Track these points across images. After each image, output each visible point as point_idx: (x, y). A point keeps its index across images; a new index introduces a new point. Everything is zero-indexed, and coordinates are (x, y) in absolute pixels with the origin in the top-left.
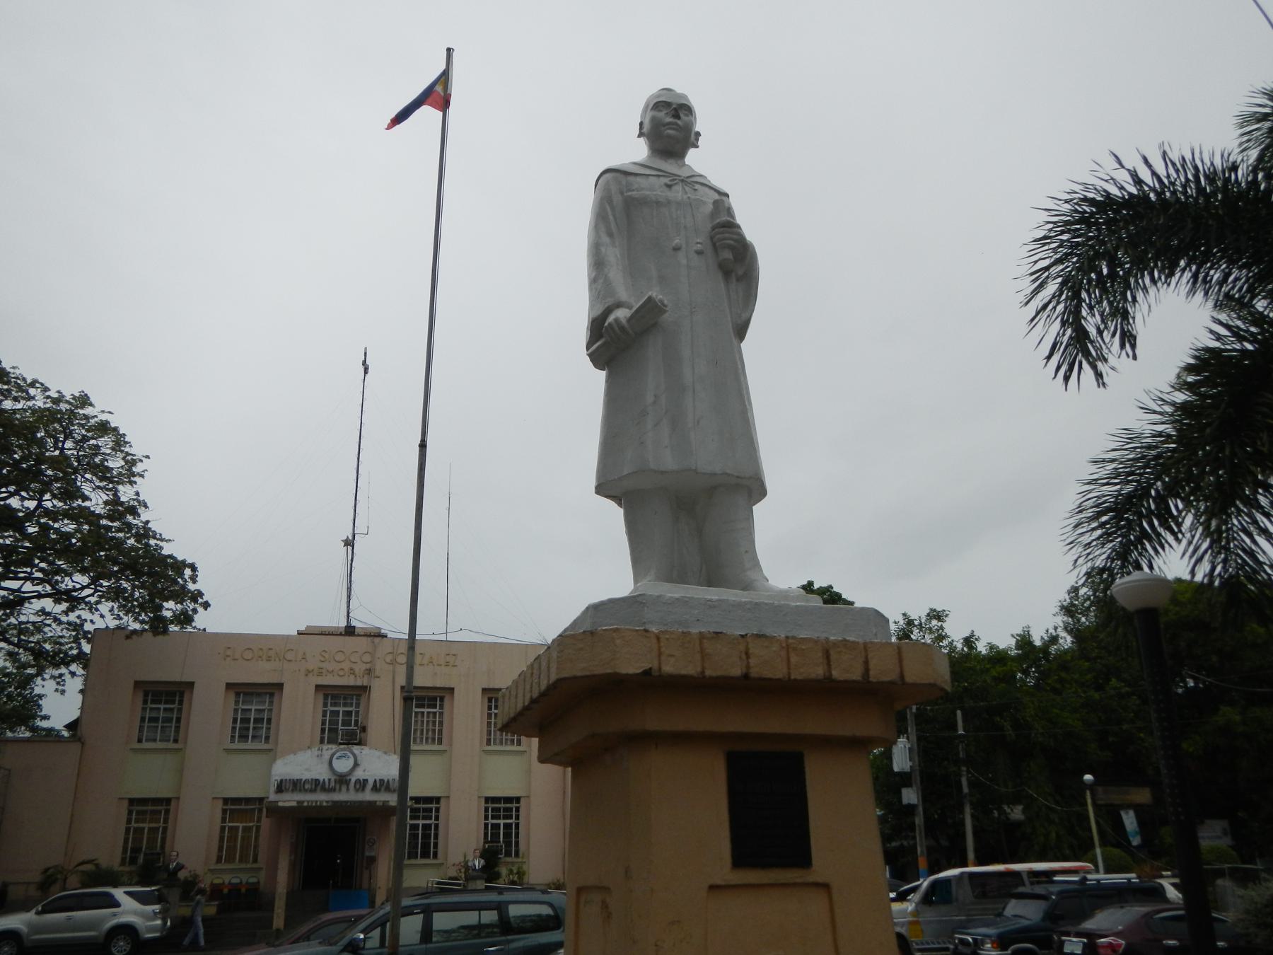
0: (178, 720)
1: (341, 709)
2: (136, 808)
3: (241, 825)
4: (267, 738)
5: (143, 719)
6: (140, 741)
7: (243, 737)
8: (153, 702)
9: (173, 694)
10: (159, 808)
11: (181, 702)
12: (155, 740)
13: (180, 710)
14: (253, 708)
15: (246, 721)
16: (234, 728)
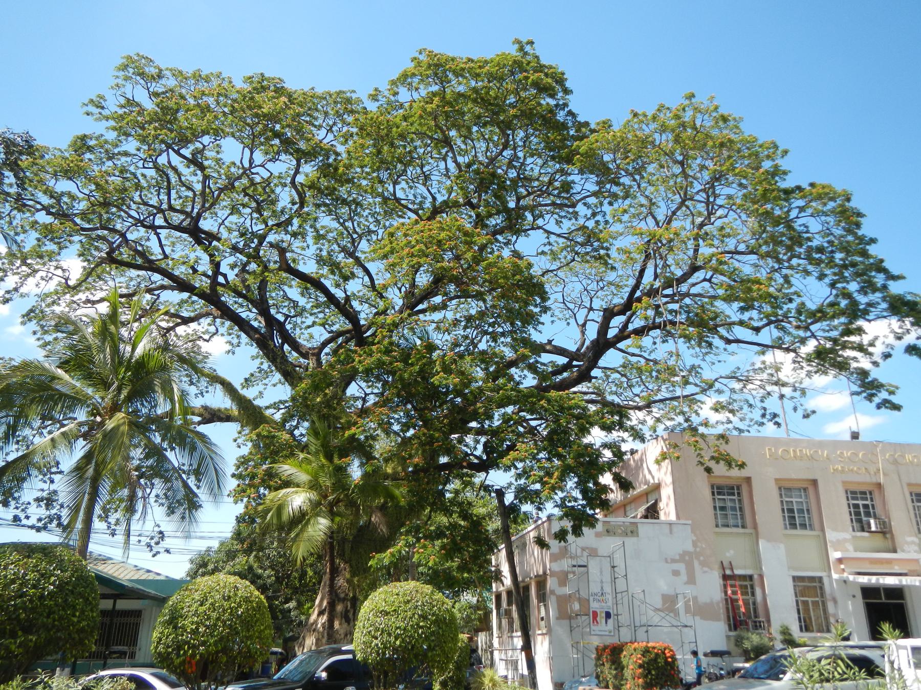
0: (741, 509)
1: (860, 503)
2: (729, 582)
3: (810, 600)
4: (810, 525)
5: (715, 508)
6: (717, 526)
7: (793, 526)
8: (719, 493)
9: (733, 488)
10: (745, 583)
11: (739, 494)
12: (728, 526)
13: (740, 501)
14: (794, 500)
15: (791, 511)
16: (784, 517)
